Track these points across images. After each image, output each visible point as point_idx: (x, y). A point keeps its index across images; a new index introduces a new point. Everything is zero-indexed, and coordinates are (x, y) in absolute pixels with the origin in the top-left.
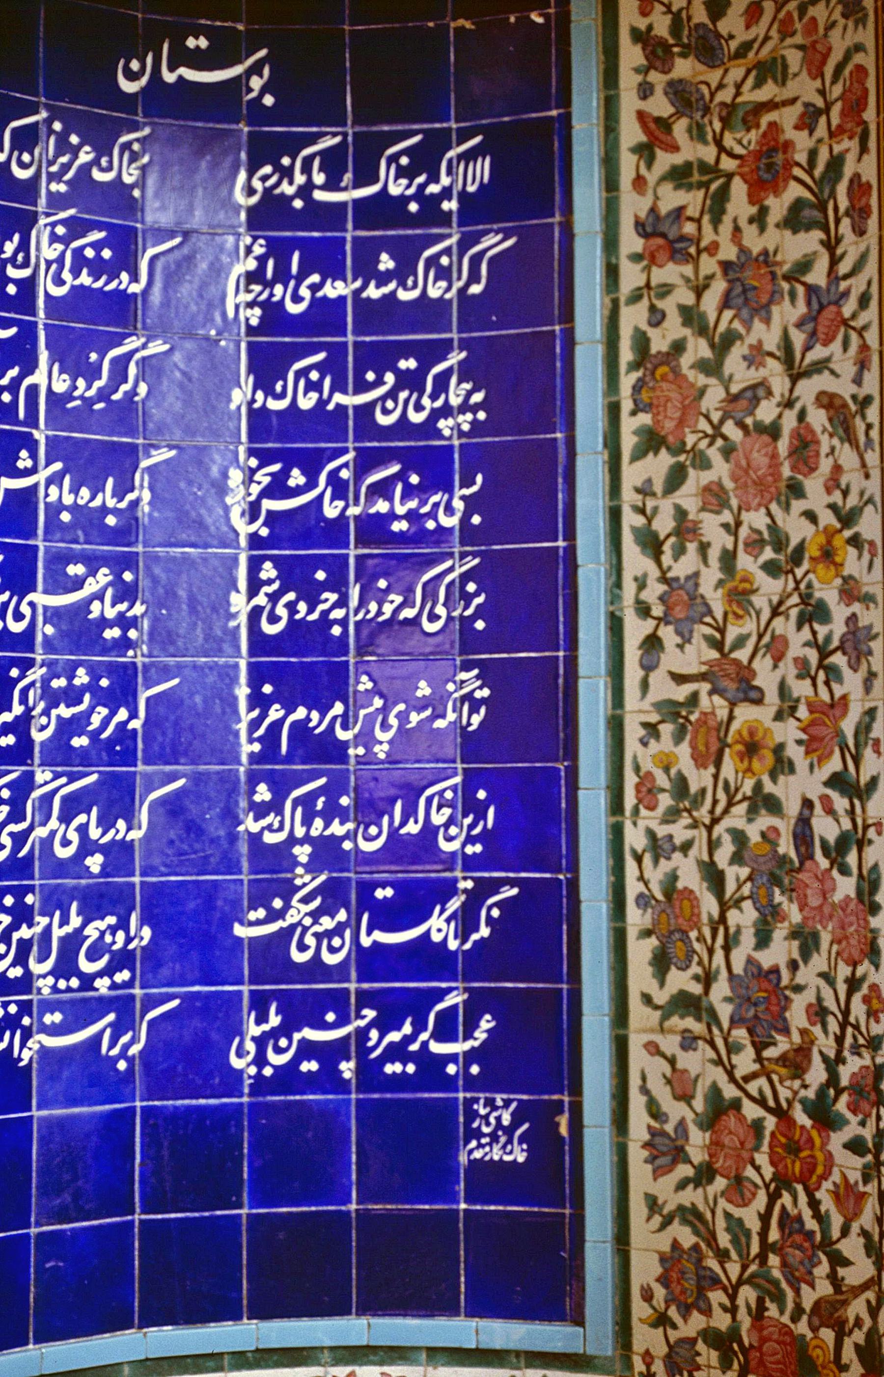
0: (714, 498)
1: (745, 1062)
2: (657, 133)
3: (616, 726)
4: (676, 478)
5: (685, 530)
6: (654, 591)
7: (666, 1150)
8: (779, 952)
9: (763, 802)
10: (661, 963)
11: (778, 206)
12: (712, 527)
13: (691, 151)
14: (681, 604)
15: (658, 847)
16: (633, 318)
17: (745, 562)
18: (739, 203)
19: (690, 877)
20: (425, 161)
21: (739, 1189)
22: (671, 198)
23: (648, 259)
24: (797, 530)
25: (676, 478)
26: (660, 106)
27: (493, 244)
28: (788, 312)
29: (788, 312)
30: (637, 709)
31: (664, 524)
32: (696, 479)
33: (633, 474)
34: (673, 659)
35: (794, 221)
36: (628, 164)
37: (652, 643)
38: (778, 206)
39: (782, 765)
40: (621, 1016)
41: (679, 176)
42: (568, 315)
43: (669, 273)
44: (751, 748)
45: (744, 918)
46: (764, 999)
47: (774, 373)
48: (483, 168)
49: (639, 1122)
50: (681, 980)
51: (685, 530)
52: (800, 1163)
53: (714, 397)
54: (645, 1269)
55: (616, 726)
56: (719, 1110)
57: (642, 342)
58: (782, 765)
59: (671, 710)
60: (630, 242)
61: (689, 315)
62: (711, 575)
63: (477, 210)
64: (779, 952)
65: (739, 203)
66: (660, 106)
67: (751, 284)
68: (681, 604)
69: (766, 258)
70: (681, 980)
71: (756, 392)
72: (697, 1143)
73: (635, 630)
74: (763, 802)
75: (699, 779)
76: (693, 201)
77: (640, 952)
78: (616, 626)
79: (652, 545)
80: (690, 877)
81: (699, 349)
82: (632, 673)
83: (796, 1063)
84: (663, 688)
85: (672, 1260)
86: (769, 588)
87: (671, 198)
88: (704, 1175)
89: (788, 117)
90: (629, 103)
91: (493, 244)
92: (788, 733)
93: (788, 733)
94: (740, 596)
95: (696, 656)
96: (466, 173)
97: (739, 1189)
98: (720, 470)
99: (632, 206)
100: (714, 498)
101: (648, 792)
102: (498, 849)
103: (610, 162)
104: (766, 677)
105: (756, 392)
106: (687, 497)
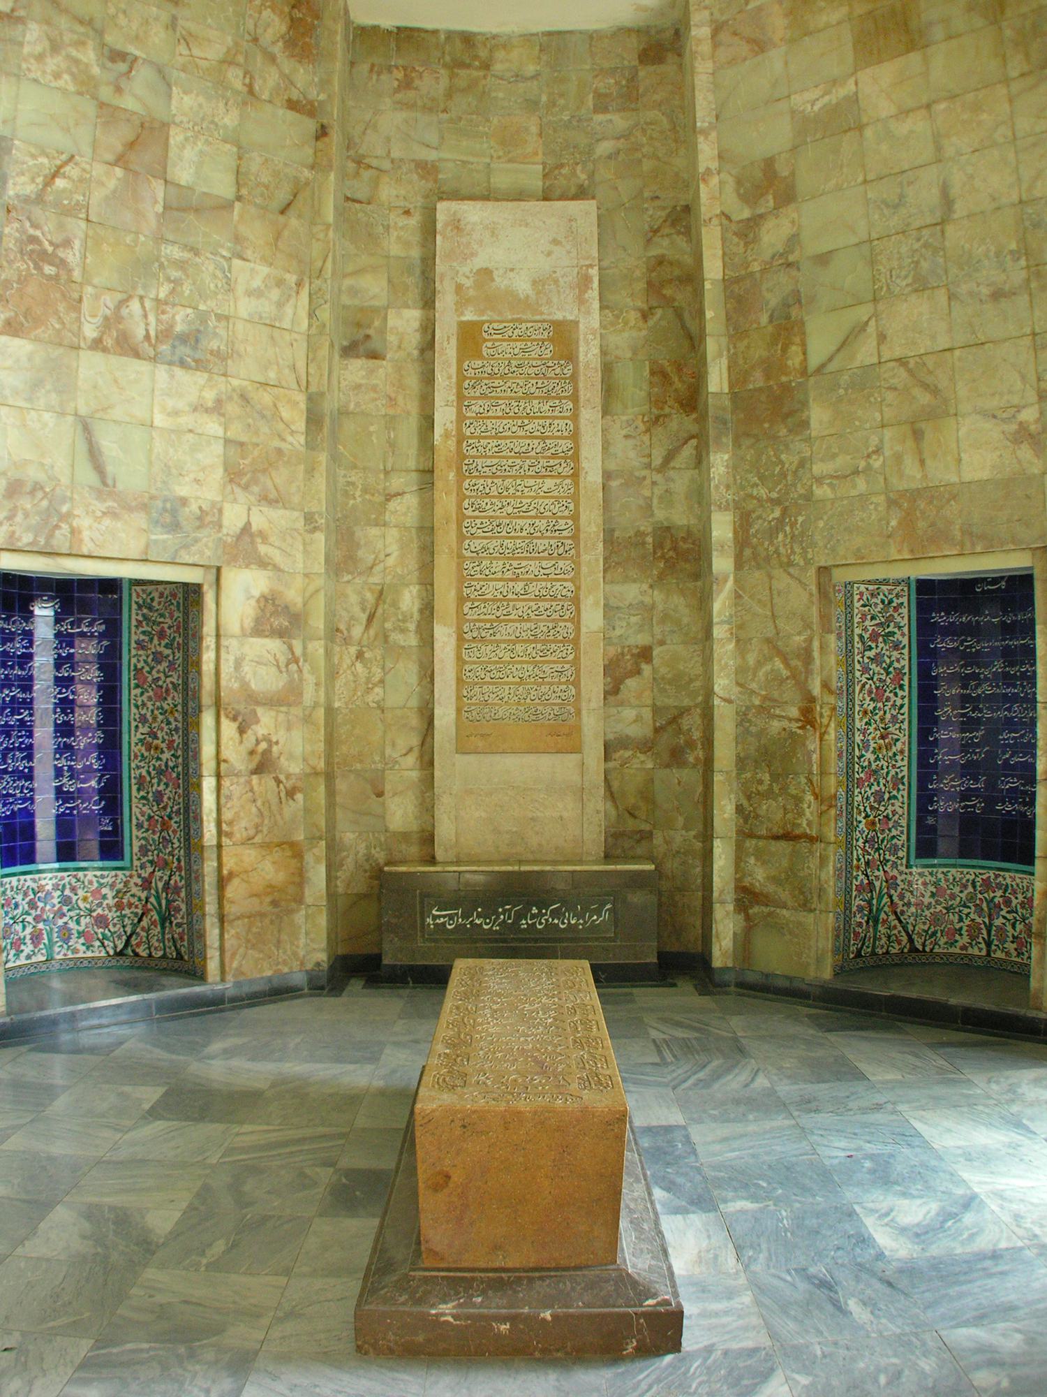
0: (150, 699)
1: (155, 808)
2: (139, 623)
3: (129, 743)
4: (142, 694)
5: (144, 704)
6: (137, 716)
7: (140, 826)
8: (162, 787)
9: (158, 759)
10: (139, 790)
11: (163, 643)
12: (149, 704)
13: (147, 628)
14: (143, 720)
15: (138, 767)
16: (134, 660)
17: (156, 712)
18: (156, 641)
19: (144, 773)
20: (91, 624)
21: (154, 833)
22: (142, 637)
23: (137, 649)
24: (166, 707)
25: (142, 694)
26: (140, 618)
27: (105, 643)
28: (165, 664)
29: (165, 664)
30: (134, 740)
31: (140, 703)
32: (146, 695)
33: (134, 692)
34: (141, 730)
35: (166, 646)
36: (133, 629)
37: (137, 727)
38: (163, 643)
39: (162, 752)
40: (130, 801)
41: (144, 633)
42: (120, 658)
43: (141, 652)
44: (156, 748)
45: (155, 781)
46: (159, 796)
47: (162, 675)
48: (103, 627)
49: (134, 822)
50: (142, 793)
51: (144, 704)
52: (165, 827)
53: (150, 679)
54: (136, 849)
55: (129, 743)
56: (150, 818)
57: (136, 669)
58: (162, 752)
59: (141, 740)
60: (133, 645)
61: (145, 662)
62: (149, 714)
63: (102, 636)
64: (162, 787)
65: (156, 641)
66: (140, 618)
67: (158, 658)
68: (143, 720)
69: (160, 653)
70: (142, 793)
71: (158, 679)
72: (146, 824)
73: (134, 724)
74: (158, 759)
75: (146, 754)
76: (147, 638)
77: (134, 788)
78: (130, 723)
79: (137, 707)
80: (144, 773)
81: (147, 669)
82: (133, 732)
83: (165, 808)
84: (139, 736)
85: (141, 847)
86: (160, 717)
87: (142, 637)
88: (147, 830)
89: (166, 626)
90: (134, 616)
91: (105, 643)
92: (164, 746)
93: (164, 746)
94: (155, 719)
95: (146, 730)
96: (99, 628)
97: (154, 833)
98: (151, 693)
99: (134, 638)
100: (150, 699)
101: (136, 756)
102: (105, 768)
103: (129, 628)
104: (160, 734)
105: (158, 679)
106: (145, 698)
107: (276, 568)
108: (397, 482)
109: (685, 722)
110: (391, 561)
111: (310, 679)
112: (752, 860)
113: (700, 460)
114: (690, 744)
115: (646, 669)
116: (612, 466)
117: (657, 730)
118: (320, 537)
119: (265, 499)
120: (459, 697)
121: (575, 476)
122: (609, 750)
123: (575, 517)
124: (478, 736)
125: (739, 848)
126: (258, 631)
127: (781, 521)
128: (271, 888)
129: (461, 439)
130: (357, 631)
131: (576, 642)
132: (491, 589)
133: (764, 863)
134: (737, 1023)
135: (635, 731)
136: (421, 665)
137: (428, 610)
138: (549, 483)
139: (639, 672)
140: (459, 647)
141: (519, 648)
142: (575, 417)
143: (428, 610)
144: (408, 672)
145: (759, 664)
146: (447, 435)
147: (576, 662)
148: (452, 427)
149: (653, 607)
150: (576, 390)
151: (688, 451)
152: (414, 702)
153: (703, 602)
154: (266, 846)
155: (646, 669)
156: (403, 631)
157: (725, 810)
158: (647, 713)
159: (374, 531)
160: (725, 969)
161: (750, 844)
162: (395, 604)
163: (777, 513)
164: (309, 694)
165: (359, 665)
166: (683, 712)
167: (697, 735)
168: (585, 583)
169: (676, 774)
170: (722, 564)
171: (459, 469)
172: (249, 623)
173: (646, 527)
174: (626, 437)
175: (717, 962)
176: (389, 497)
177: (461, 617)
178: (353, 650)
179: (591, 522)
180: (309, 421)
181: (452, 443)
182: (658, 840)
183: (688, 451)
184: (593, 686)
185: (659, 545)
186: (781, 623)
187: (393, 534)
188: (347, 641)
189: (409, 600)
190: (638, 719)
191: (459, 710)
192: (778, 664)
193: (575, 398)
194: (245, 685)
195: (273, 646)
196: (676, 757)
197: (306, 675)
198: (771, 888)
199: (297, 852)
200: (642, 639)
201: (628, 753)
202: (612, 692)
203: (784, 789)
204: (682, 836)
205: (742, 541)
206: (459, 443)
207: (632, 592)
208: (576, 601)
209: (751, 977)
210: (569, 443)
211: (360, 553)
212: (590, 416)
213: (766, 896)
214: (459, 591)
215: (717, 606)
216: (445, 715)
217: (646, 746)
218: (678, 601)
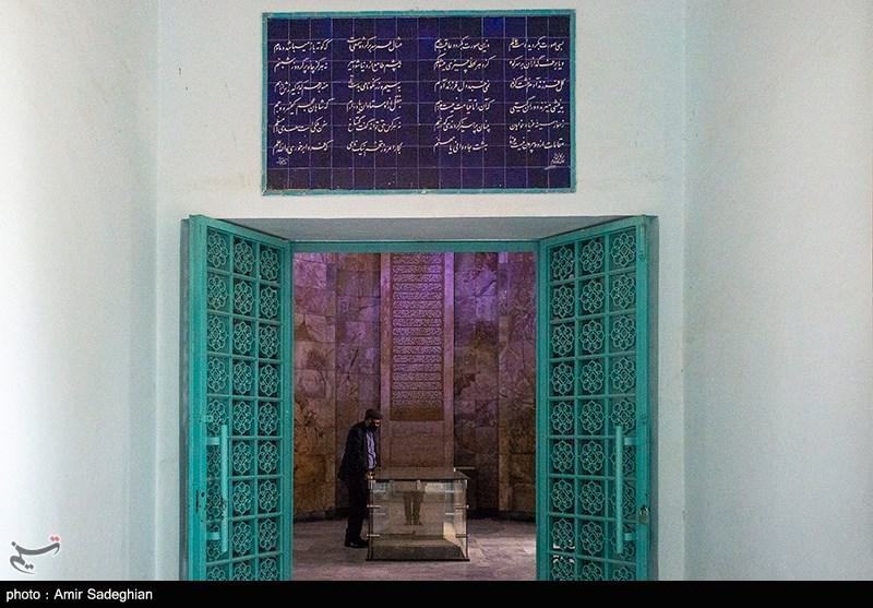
107: (316, 341)
108: (364, 302)
109: (490, 407)
110: (361, 337)
111: (329, 386)
112: (515, 464)
113: (496, 293)
114: (492, 416)
115: (472, 383)
116: (458, 294)
117: (477, 411)
118: (333, 327)
119: (310, 311)
120: (392, 396)
121: (442, 300)
122: (456, 419)
123: (442, 318)
124: (399, 415)
125: (510, 459)
126: (308, 367)
127: (527, 320)
128: (313, 474)
129: (392, 283)
130: (347, 368)
131: (442, 373)
132: (406, 350)
133: (520, 465)
134: (505, 526)
135: (467, 411)
136: (375, 383)
137: (378, 359)
138: (431, 303)
139: (469, 385)
140: (391, 375)
141: (417, 375)
142: (442, 273)
143: (378, 359)
144: (369, 386)
145: (518, 380)
146: (386, 282)
147: (442, 381)
148: (388, 278)
149: (476, 356)
150: (443, 261)
151: (492, 287)
152: (371, 398)
153: (496, 357)
154: (310, 456)
155: (472, 383)
156: (367, 367)
157: (504, 443)
158: (472, 403)
159: (354, 324)
160: (504, 512)
161: (514, 457)
162: (363, 356)
163: (526, 317)
164: (328, 395)
165: (348, 383)
166: (488, 402)
167: (494, 412)
168: (446, 347)
169: (484, 430)
170: (502, 338)
171: (391, 297)
172: (305, 363)
173: (472, 321)
174: (465, 281)
175: (501, 509)
176: (361, 309)
177: (392, 362)
178: (346, 375)
179: (449, 319)
180: (328, 276)
181: (388, 285)
182: (477, 458)
183: (492, 287)
184: (449, 393)
185: (478, 330)
186: (526, 364)
187: (362, 325)
188: (343, 372)
189: (369, 354)
190: (469, 405)
191: (391, 402)
192: (525, 380)
193: (442, 264)
194: (303, 389)
195: (315, 373)
196: (485, 422)
197: (328, 384)
198: (523, 475)
199: (324, 461)
200: (471, 371)
201: (464, 421)
202: (457, 394)
203: (528, 433)
204: (486, 457)
205: (511, 330)
206: (391, 286)
207: (466, 350)
208: (442, 354)
209: (516, 515)
210: (440, 285)
211: (348, 333)
212: (449, 272)
213: (520, 478)
214: (392, 350)
215: (500, 357)
216: (385, 404)
217: (471, 417)
218: (488, 354)
